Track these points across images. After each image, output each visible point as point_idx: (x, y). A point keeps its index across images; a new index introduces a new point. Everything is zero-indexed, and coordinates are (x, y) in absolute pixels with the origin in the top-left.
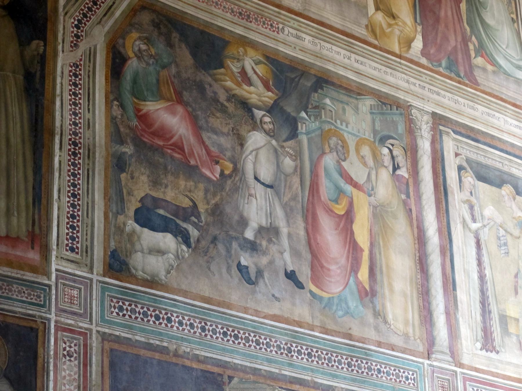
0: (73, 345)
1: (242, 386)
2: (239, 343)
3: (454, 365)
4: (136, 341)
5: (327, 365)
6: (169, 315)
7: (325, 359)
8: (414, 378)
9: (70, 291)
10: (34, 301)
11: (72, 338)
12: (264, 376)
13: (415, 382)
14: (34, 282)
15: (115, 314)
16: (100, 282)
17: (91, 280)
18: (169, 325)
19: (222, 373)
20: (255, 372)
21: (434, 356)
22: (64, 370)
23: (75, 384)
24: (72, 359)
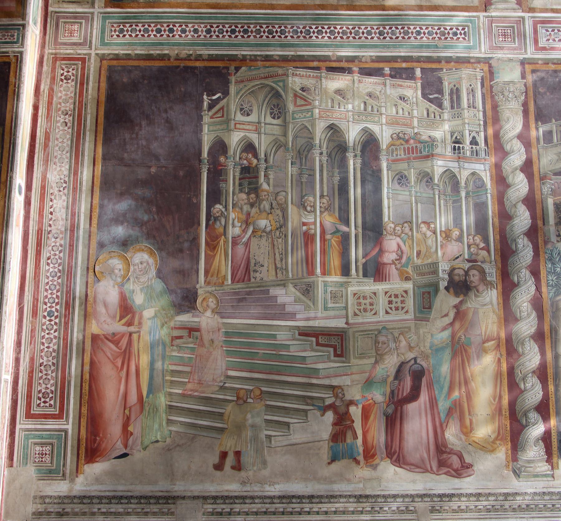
0: (70, 70)
1: (250, 73)
2: (249, 36)
3: (521, 11)
4: (136, 54)
5: (354, 38)
6: (171, 26)
7: (351, 33)
8: (465, 33)
9: (70, 27)
10: (8, 40)
11: (70, 64)
12: (276, 61)
14: (9, 25)
15: (115, 36)
16: (101, 13)
17: (92, 13)
18: (171, 35)
19: (228, 65)
20: (267, 58)
21: (493, 7)
22: (61, 91)
23: (71, 101)
24: (69, 81)
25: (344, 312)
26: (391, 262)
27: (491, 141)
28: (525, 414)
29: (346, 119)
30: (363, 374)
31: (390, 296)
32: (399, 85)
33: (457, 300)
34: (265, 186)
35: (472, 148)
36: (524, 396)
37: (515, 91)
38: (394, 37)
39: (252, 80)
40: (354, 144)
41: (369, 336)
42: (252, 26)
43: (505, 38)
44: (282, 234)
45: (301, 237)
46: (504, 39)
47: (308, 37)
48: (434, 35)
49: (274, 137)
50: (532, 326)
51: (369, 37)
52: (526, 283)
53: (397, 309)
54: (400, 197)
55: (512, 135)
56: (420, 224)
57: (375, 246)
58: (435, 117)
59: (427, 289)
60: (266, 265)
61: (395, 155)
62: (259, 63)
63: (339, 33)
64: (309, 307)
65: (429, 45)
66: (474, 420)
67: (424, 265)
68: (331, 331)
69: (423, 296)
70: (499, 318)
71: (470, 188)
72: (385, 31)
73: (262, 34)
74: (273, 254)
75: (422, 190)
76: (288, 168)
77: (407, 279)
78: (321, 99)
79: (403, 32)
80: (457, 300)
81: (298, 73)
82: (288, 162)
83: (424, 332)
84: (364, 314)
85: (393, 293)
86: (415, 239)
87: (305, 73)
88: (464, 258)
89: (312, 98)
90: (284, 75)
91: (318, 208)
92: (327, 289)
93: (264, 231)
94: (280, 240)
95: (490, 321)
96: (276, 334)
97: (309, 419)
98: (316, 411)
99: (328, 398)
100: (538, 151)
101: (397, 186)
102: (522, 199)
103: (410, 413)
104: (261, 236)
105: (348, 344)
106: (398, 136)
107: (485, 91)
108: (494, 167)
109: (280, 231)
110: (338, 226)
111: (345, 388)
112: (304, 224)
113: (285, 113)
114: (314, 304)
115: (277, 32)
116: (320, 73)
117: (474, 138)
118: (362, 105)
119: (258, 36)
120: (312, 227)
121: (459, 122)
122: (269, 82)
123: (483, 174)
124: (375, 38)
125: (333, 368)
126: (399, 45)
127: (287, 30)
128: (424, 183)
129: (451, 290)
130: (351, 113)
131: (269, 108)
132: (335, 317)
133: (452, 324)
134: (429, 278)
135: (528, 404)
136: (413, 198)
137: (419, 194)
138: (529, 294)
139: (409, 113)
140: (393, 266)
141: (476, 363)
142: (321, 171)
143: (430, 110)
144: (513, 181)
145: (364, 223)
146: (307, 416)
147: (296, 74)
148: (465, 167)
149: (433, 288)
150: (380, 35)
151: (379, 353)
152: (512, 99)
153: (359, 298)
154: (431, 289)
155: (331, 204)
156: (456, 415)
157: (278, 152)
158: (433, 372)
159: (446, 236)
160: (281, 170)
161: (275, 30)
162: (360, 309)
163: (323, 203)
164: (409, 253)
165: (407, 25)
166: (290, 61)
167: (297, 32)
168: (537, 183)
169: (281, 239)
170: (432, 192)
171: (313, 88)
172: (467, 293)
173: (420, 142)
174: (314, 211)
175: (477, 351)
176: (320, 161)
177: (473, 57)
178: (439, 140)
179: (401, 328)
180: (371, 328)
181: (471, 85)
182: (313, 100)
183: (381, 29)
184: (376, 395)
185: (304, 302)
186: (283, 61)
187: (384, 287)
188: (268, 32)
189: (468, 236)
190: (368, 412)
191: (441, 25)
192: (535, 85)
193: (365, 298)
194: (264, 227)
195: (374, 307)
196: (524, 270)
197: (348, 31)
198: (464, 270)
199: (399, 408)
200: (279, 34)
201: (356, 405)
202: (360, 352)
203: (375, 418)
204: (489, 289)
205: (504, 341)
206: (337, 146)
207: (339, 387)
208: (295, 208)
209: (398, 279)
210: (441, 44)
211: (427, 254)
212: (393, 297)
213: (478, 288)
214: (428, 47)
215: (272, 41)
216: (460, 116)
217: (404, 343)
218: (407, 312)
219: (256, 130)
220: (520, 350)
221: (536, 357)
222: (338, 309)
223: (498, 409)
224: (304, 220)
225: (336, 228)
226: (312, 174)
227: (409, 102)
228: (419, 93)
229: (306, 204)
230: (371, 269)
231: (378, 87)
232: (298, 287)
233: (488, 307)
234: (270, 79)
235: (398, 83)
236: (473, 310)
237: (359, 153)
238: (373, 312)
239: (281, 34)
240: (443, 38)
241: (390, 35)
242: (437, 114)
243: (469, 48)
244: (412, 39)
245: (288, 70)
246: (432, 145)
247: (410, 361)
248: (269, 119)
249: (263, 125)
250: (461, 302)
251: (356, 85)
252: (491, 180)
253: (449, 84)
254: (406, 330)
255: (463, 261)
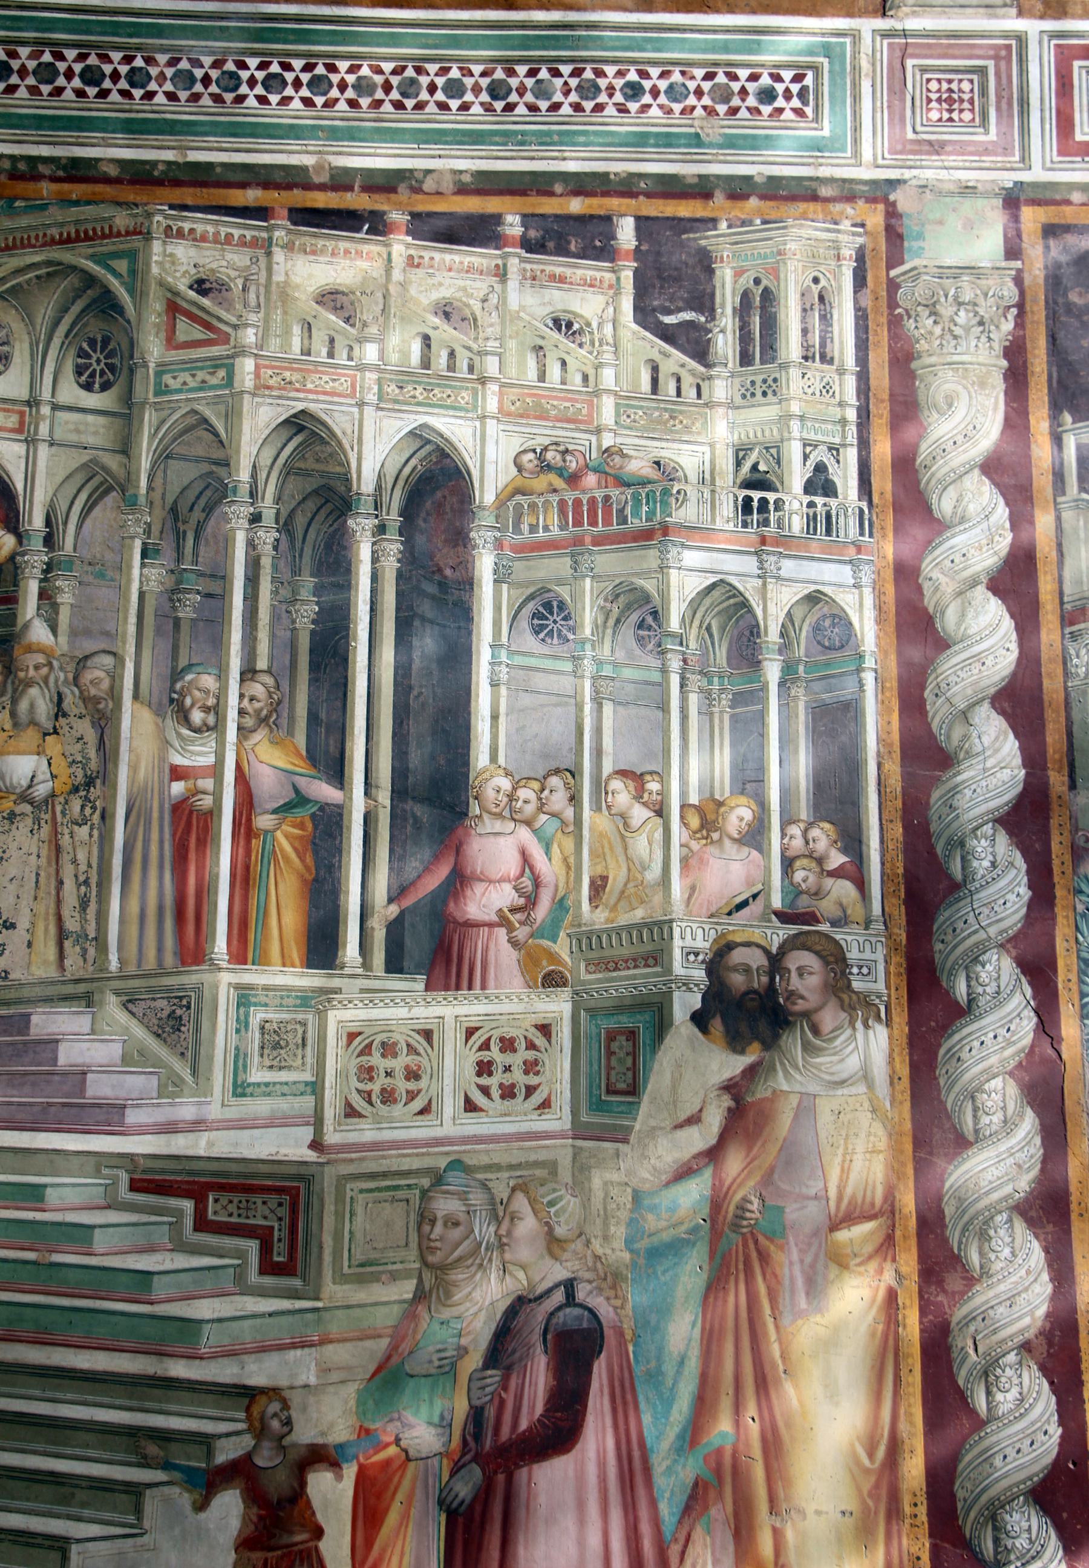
3: (1014, 11)
5: (399, 106)
7: (387, 87)
12: (107, 180)
13: (805, 103)
25: (309, 1101)
26: (494, 918)
27: (883, 483)
28: (993, 1515)
29: (353, 395)
30: (368, 1344)
31: (486, 1046)
32: (552, 277)
33: (735, 1065)
34: (40, 633)
35: (811, 505)
36: (986, 1443)
37: (981, 300)
38: (544, 105)
39: (15, 247)
40: (379, 487)
41: (400, 1194)
42: (24, 52)
43: (950, 111)
44: (94, 808)
45: (161, 818)
46: (946, 116)
47: (229, 97)
48: (692, 100)
49: (85, 457)
50: (1019, 1166)
51: (454, 104)
52: (1000, 1004)
53: (508, 1093)
54: (540, 681)
55: (964, 458)
56: (609, 777)
57: (437, 858)
58: (679, 394)
59: (626, 1021)
60: (23, 923)
61: (525, 528)
62: (46, 188)
63: (343, 86)
64: (178, 1082)
65: (668, 135)
66: (790, 1535)
67: (618, 931)
68: (253, 1175)
69: (608, 1047)
70: (894, 1135)
71: (800, 651)
72: (514, 82)
73: (61, 81)
74: (53, 883)
75: (620, 655)
76: (130, 567)
77: (553, 981)
78: (266, 321)
79: (579, 88)
80: (735, 1065)
81: (187, 226)
82: (131, 548)
83: (605, 1184)
84: (383, 1110)
85: (496, 1034)
86: (586, 833)
87: (211, 229)
88: (768, 905)
89: (234, 320)
90: (136, 233)
91: (232, 715)
92: (247, 1015)
93: (25, 797)
94: (83, 832)
95: (860, 1146)
96: (45, 1186)
97: (147, 1524)
98: (176, 1490)
99: (228, 1435)
100: (1058, 519)
101: (530, 642)
102: (992, 691)
103: (542, 1499)
104: (12, 817)
105: (314, 1227)
106: (541, 458)
107: (867, 301)
108: (889, 574)
109: (87, 799)
110: (302, 782)
111: (295, 1399)
112: (177, 773)
113: (132, 371)
114: (194, 1072)
115: (115, 76)
116: (267, 229)
117: (820, 468)
118: (416, 347)
119: (46, 89)
120: (208, 784)
121: (768, 412)
122: (80, 258)
123: (847, 600)
124: (476, 109)
125: (254, 1316)
126: (560, 133)
127: (154, 71)
128: (628, 631)
129: (717, 1025)
130: (371, 376)
131: (73, 352)
132: (273, 1122)
133: (713, 1154)
134: (634, 977)
135: (1005, 1476)
136: (587, 684)
137: (607, 671)
138: (1010, 1043)
139: (585, 378)
140: (501, 933)
141: (802, 1303)
142: (252, 580)
143: (663, 369)
144: (959, 624)
145: (400, 773)
146: (138, 1511)
147: (180, 231)
148: (783, 573)
149: (647, 1017)
150: (495, 97)
151: (431, 1259)
152: (967, 329)
153: (367, 1050)
154: (640, 1022)
155: (279, 703)
156: (720, 1512)
157: (97, 511)
158: (636, 1337)
159: (702, 827)
160: (101, 575)
161: (108, 69)
162: (369, 1093)
163: (252, 699)
164: (561, 885)
165: (593, 60)
166: (159, 182)
167: (192, 80)
168: (1050, 634)
169: (85, 829)
170: (657, 663)
171: (240, 282)
172: (776, 1037)
173: (622, 483)
174: (218, 728)
175: (808, 1259)
176: (251, 544)
177: (831, 181)
178: (693, 477)
179: (519, 1166)
180: (406, 1164)
181: (816, 280)
182: (235, 327)
183: (499, 74)
184: (411, 1427)
185: (158, 1063)
186: (133, 182)
187: (463, 1010)
188: (82, 76)
189: (785, 824)
190: (379, 1496)
191: (716, 64)
192: (1055, 281)
193: (389, 1049)
194: (25, 783)
195: (423, 1083)
196: (992, 956)
197: (379, 79)
198: (766, 952)
199: (501, 1478)
200: (123, 84)
201: (335, 1465)
202: (359, 1257)
203: (405, 1517)
204: (859, 1025)
205: (913, 1223)
206: (316, 492)
207: (273, 1392)
208: (146, 715)
209: (518, 980)
210: (714, 130)
211: (631, 889)
212: (495, 1048)
213: (816, 1018)
214: (667, 140)
215: (98, 111)
216: (771, 389)
217: (528, 1225)
218: (546, 1105)
219: (19, 430)
220: (974, 1257)
221: (1037, 1288)
222: (285, 1089)
223: (884, 1492)
224: (178, 760)
225: (297, 790)
226: (219, 591)
227: (586, 339)
228: (627, 304)
229: (188, 701)
230: (416, 945)
231: (478, 284)
232: (138, 1009)
233: (853, 1090)
234: (84, 248)
235: (549, 269)
236: (794, 1100)
237: (393, 517)
238: (418, 1104)
239: (133, 85)
240: (722, 109)
241: (529, 97)
242: (688, 381)
243: (818, 146)
244: (610, 110)
245: (149, 215)
246: (666, 492)
247: (549, 1292)
248: (70, 392)
249: (46, 410)
250: (751, 1071)
251: (397, 275)
252: (879, 621)
253: (738, 274)
254: (538, 1172)
255: (764, 918)
